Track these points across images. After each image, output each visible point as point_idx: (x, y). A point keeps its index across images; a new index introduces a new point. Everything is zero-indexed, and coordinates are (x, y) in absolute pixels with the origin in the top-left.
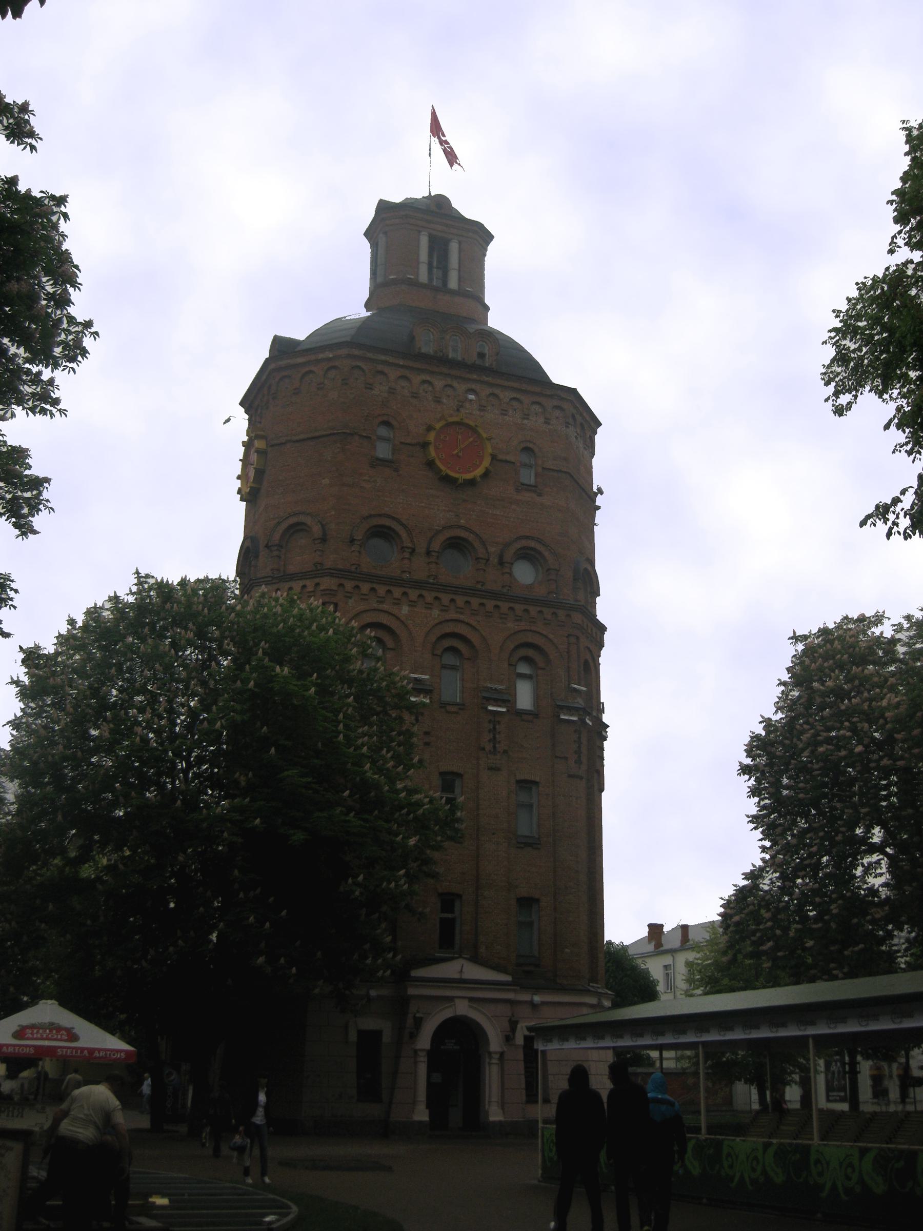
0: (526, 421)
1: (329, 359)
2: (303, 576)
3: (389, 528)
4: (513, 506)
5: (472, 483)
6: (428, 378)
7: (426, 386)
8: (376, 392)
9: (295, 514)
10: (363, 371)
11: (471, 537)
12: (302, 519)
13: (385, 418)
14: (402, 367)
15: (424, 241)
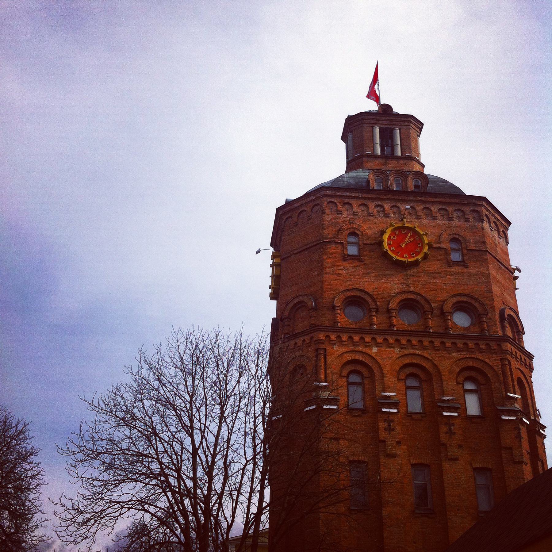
0: (451, 222)
1: (314, 200)
2: (303, 333)
3: (359, 297)
4: (449, 276)
5: (416, 264)
6: (379, 203)
7: (379, 208)
8: (345, 215)
9: (297, 297)
10: (335, 203)
11: (418, 298)
12: (301, 299)
13: (352, 230)
14: (361, 198)
15: (377, 130)
